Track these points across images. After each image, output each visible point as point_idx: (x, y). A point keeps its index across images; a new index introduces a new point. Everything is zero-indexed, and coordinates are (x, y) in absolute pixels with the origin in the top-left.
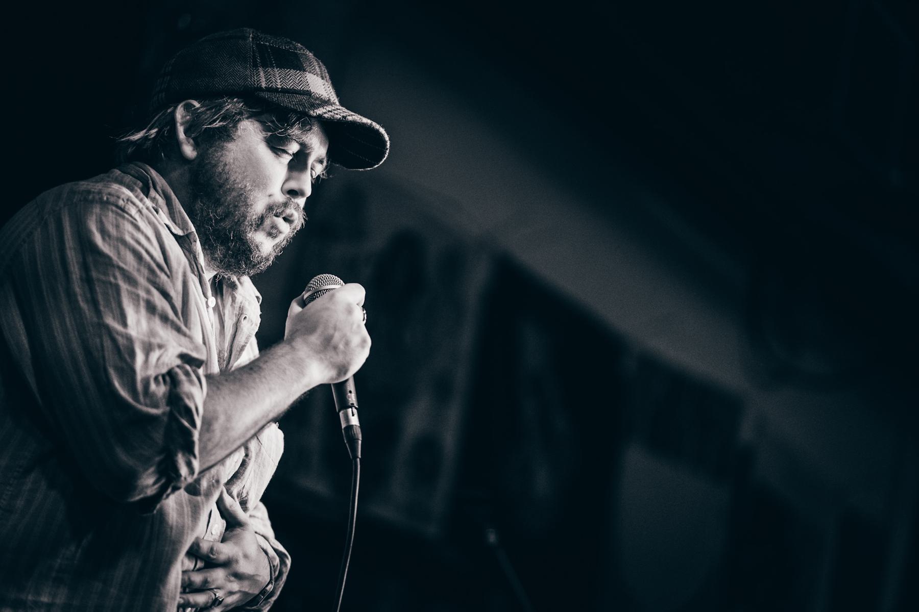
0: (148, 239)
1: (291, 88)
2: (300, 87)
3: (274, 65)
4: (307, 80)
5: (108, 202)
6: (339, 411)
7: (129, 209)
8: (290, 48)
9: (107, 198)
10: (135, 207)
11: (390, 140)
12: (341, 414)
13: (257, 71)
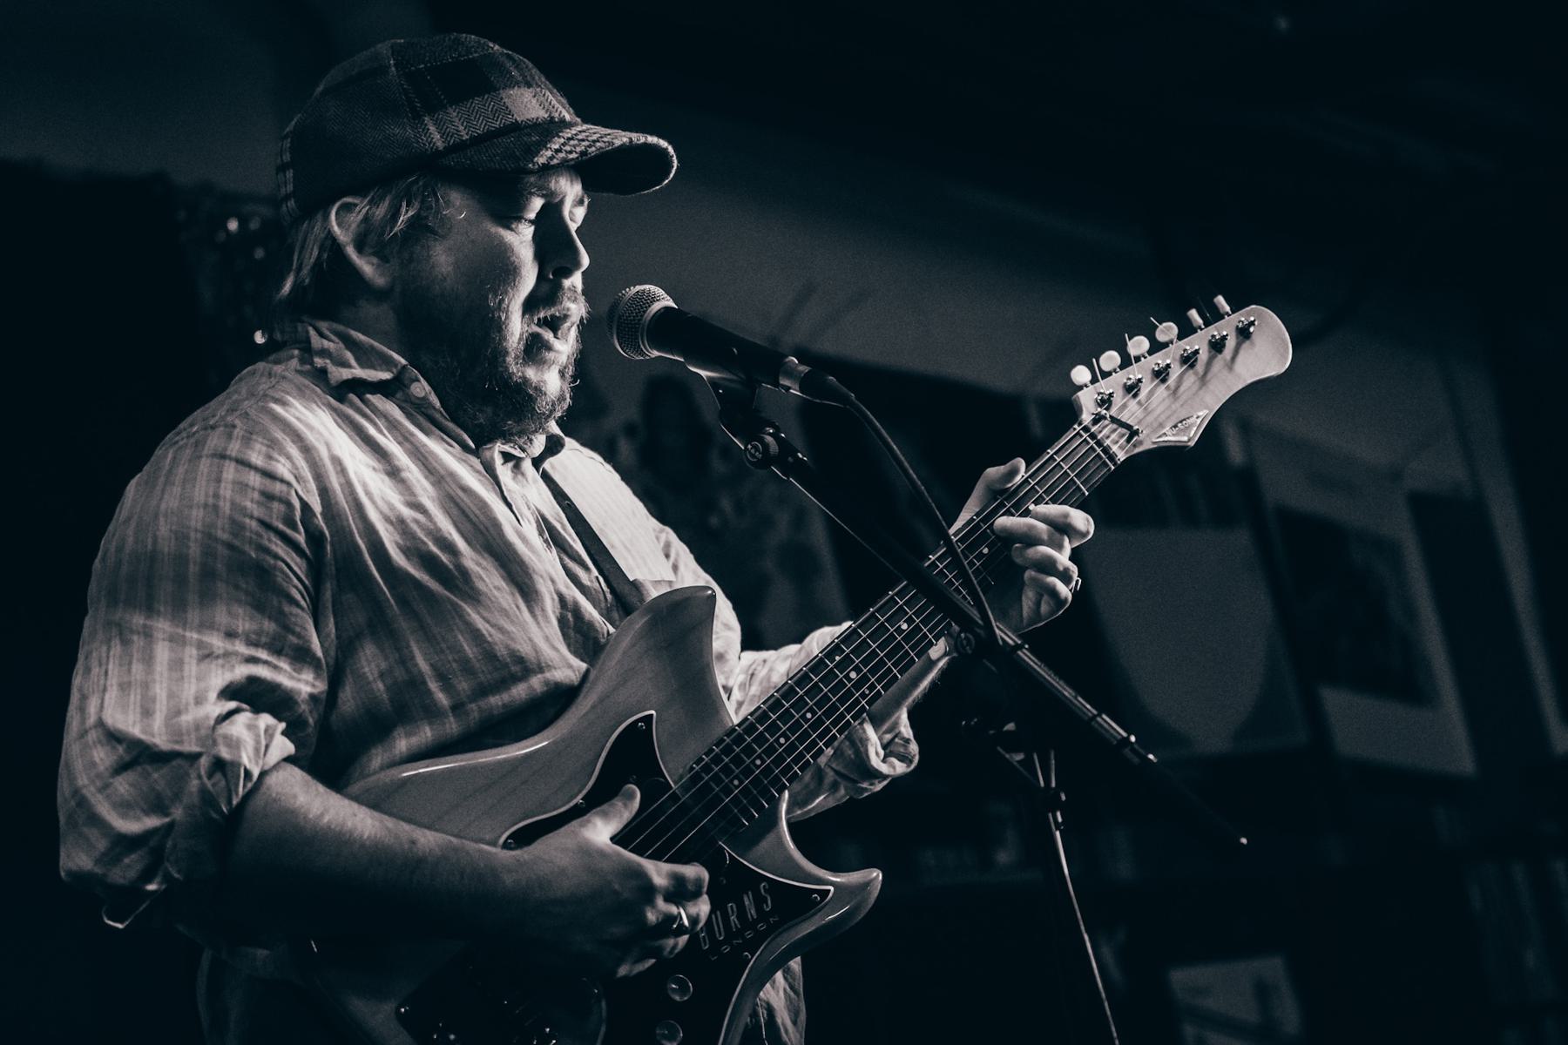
13: (422, 124)
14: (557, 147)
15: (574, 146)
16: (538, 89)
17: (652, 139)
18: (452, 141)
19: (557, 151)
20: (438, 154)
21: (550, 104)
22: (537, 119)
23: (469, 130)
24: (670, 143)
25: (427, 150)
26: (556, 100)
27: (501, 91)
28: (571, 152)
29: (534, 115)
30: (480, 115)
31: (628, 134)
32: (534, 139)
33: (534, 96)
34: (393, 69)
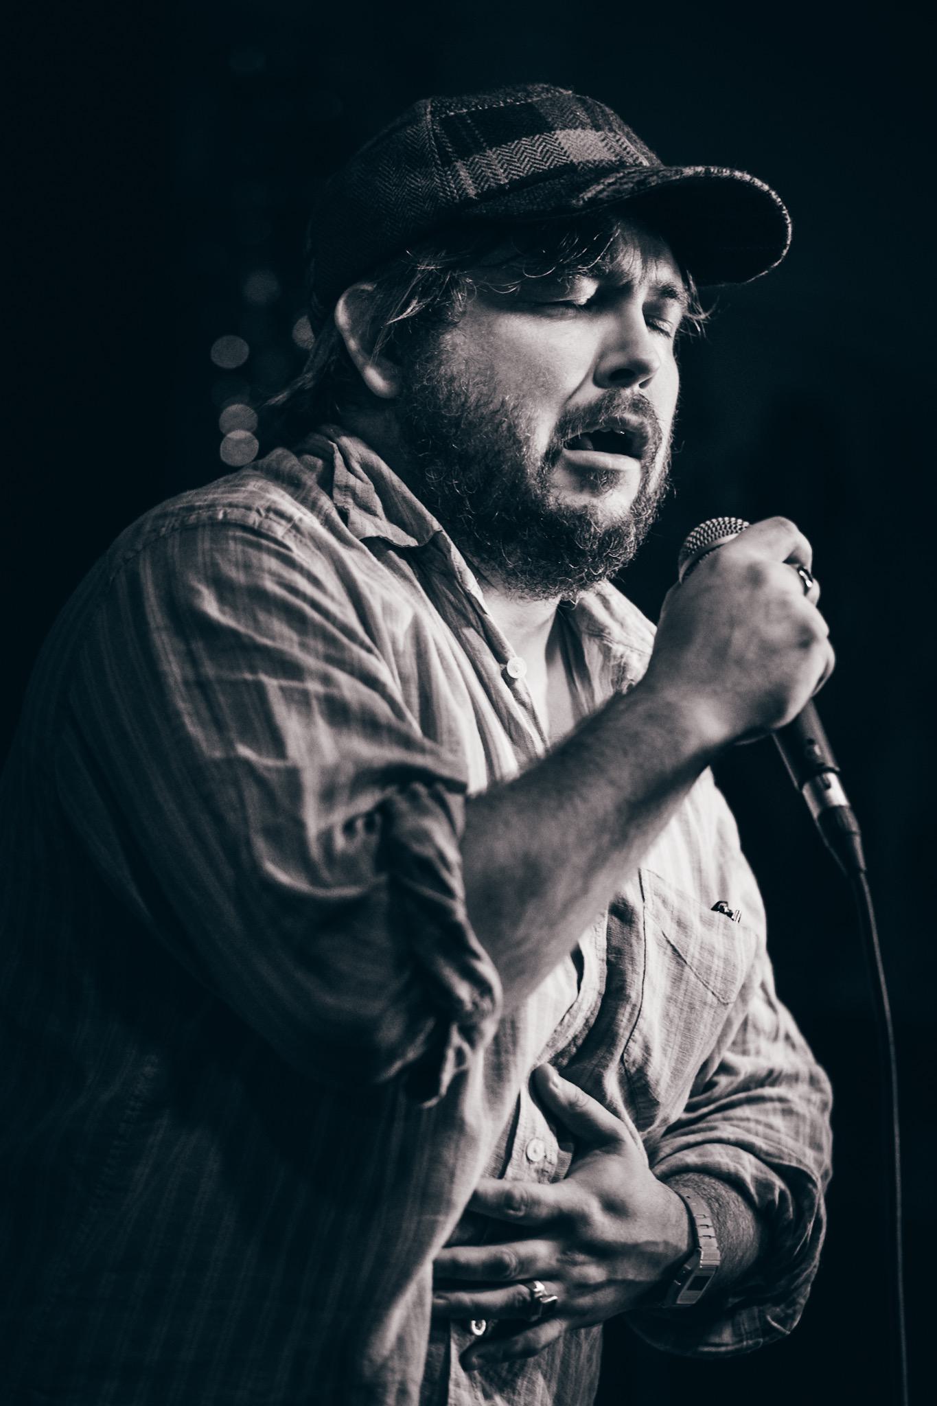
0: (315, 581)
1: (530, 173)
2: (548, 164)
3: (484, 145)
4: (562, 145)
5: (226, 524)
6: (801, 787)
7: (270, 528)
9: (225, 514)
10: (283, 522)
11: (772, 187)
12: (806, 792)
16: (611, 135)
18: (486, 186)
20: (467, 201)
21: (625, 149)
22: (602, 161)
23: (509, 173)
25: (455, 198)
27: (558, 132)
30: (526, 157)
33: (603, 140)
34: (429, 117)
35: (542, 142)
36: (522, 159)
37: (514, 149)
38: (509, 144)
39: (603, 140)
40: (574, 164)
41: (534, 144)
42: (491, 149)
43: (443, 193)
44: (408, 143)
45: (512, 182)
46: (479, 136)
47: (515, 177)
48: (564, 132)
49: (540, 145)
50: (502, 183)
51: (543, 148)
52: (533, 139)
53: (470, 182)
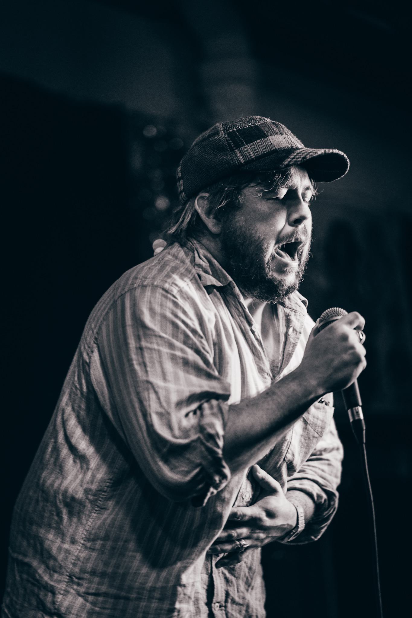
1: (262, 154)
2: (268, 150)
3: (244, 143)
4: (271, 142)
8: (252, 124)
14: (293, 157)
15: (300, 156)
17: (336, 151)
18: (247, 159)
19: (293, 158)
20: (241, 165)
21: (292, 141)
22: (286, 147)
23: (255, 154)
24: (345, 153)
25: (236, 164)
26: (295, 140)
27: (269, 137)
28: (298, 158)
29: (284, 146)
31: (324, 149)
32: (283, 155)
33: (284, 139)
34: (222, 132)
35: (264, 141)
36: (258, 148)
37: (255, 144)
38: (253, 142)
39: (284, 139)
40: (276, 149)
41: (262, 142)
42: (247, 145)
43: (232, 162)
44: (217, 142)
45: (256, 157)
46: (242, 140)
47: (257, 155)
48: (271, 137)
49: (264, 143)
50: (253, 157)
51: (265, 144)
52: (261, 140)
53: (242, 157)
